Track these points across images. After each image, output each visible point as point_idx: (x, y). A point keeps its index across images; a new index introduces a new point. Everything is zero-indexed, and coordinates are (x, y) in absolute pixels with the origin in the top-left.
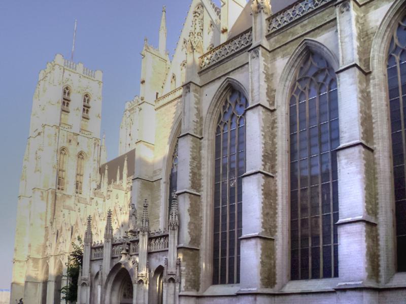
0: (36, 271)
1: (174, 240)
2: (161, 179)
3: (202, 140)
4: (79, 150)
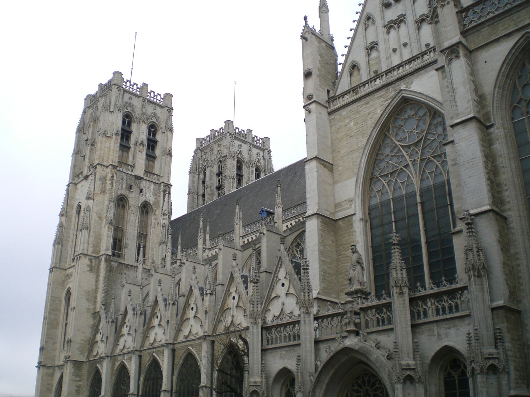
0: (78, 381)
1: (483, 295)
2: (355, 214)
3: (492, 130)
4: (142, 199)
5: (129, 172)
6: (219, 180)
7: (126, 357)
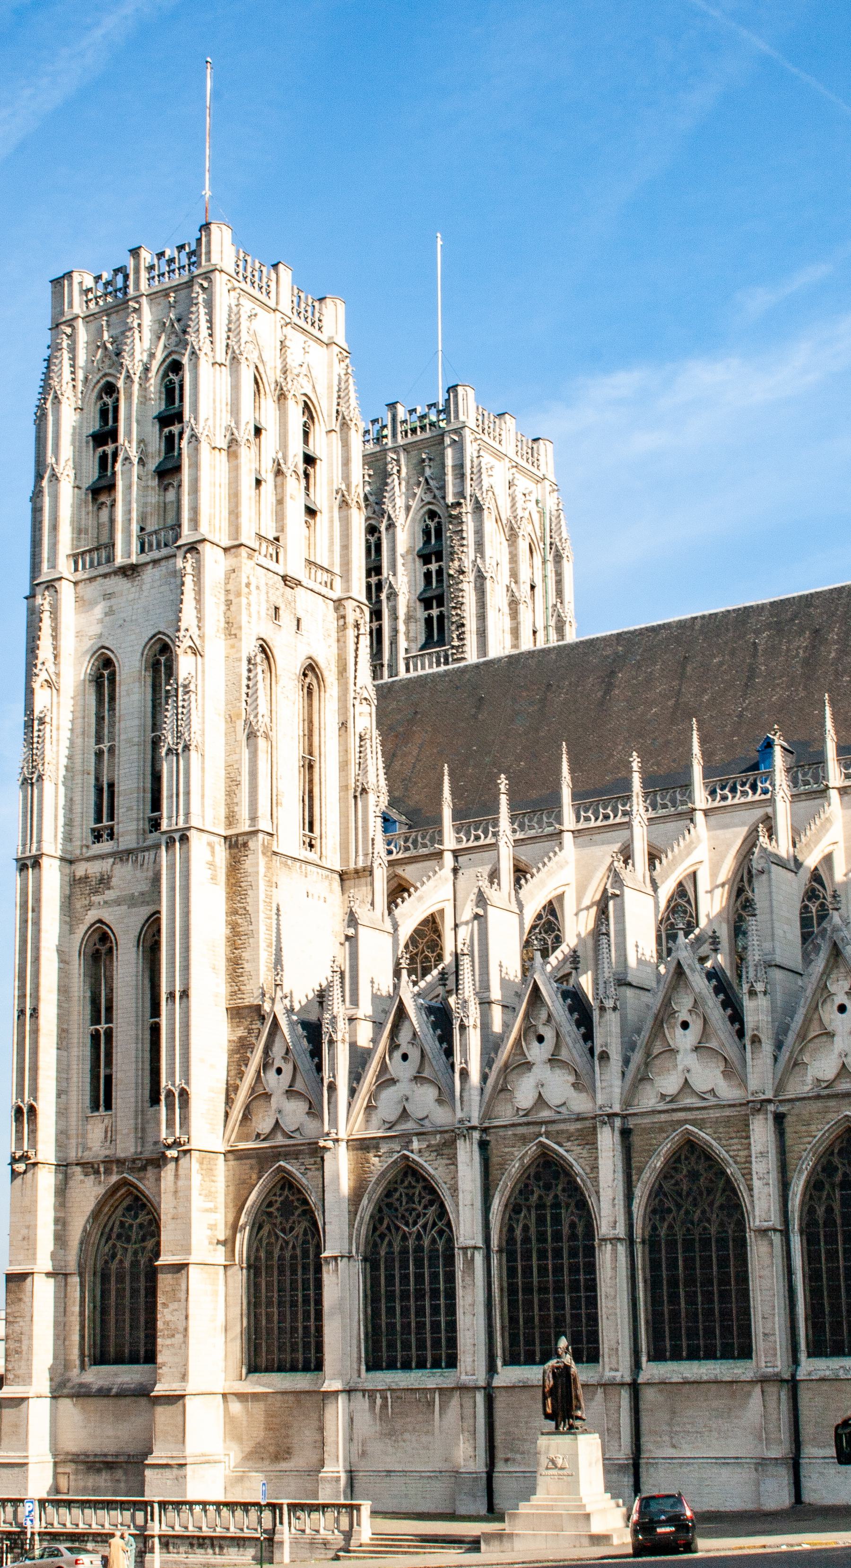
5: (272, 565)
6: (428, 575)
7: (415, 1145)
